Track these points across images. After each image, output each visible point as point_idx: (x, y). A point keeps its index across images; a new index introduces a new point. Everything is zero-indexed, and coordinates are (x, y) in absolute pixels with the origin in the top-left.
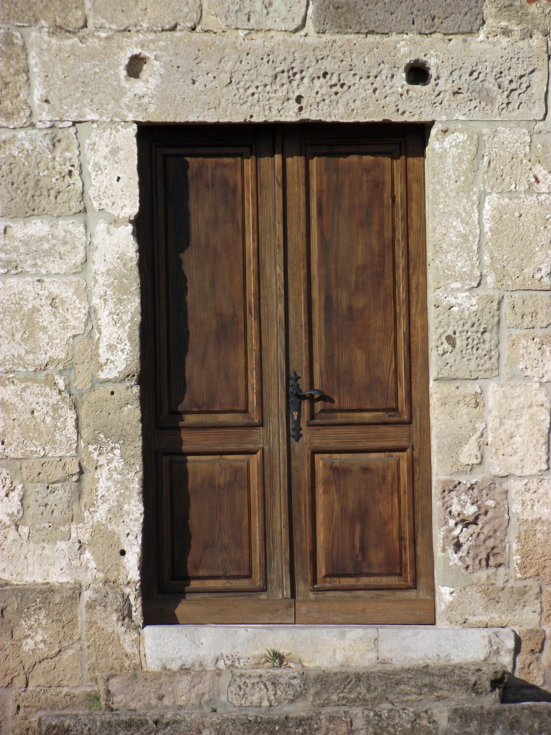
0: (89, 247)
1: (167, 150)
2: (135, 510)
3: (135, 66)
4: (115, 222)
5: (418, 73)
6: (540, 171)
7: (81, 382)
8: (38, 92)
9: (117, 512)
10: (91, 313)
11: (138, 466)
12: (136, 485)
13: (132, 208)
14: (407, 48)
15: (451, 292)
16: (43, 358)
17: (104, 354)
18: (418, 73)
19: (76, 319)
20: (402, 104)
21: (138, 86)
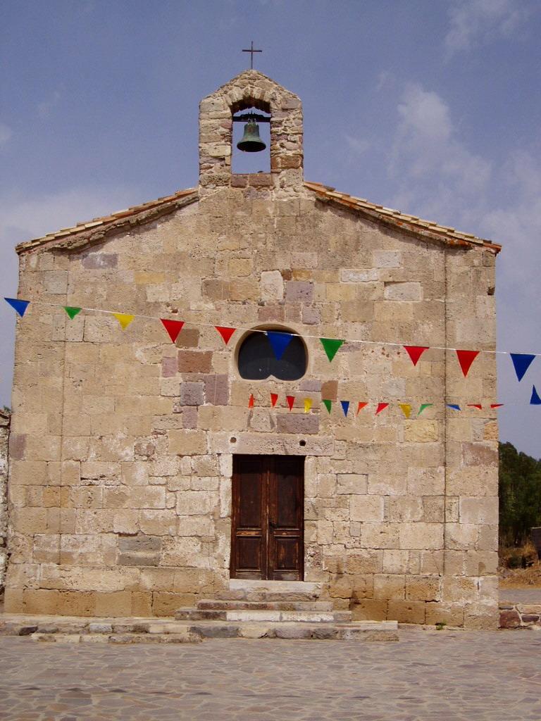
0: (219, 484)
1: (241, 462)
2: (228, 550)
3: (233, 440)
4: (225, 478)
5: (303, 443)
6: (332, 468)
7: (216, 518)
8: (209, 446)
9: (223, 550)
10: (220, 501)
11: (230, 539)
12: (229, 544)
13: (231, 475)
14: (300, 437)
15: (309, 500)
16: (207, 512)
17: (222, 510)
18: (303, 443)
19: (215, 502)
20: (296, 450)
21: (233, 445)
